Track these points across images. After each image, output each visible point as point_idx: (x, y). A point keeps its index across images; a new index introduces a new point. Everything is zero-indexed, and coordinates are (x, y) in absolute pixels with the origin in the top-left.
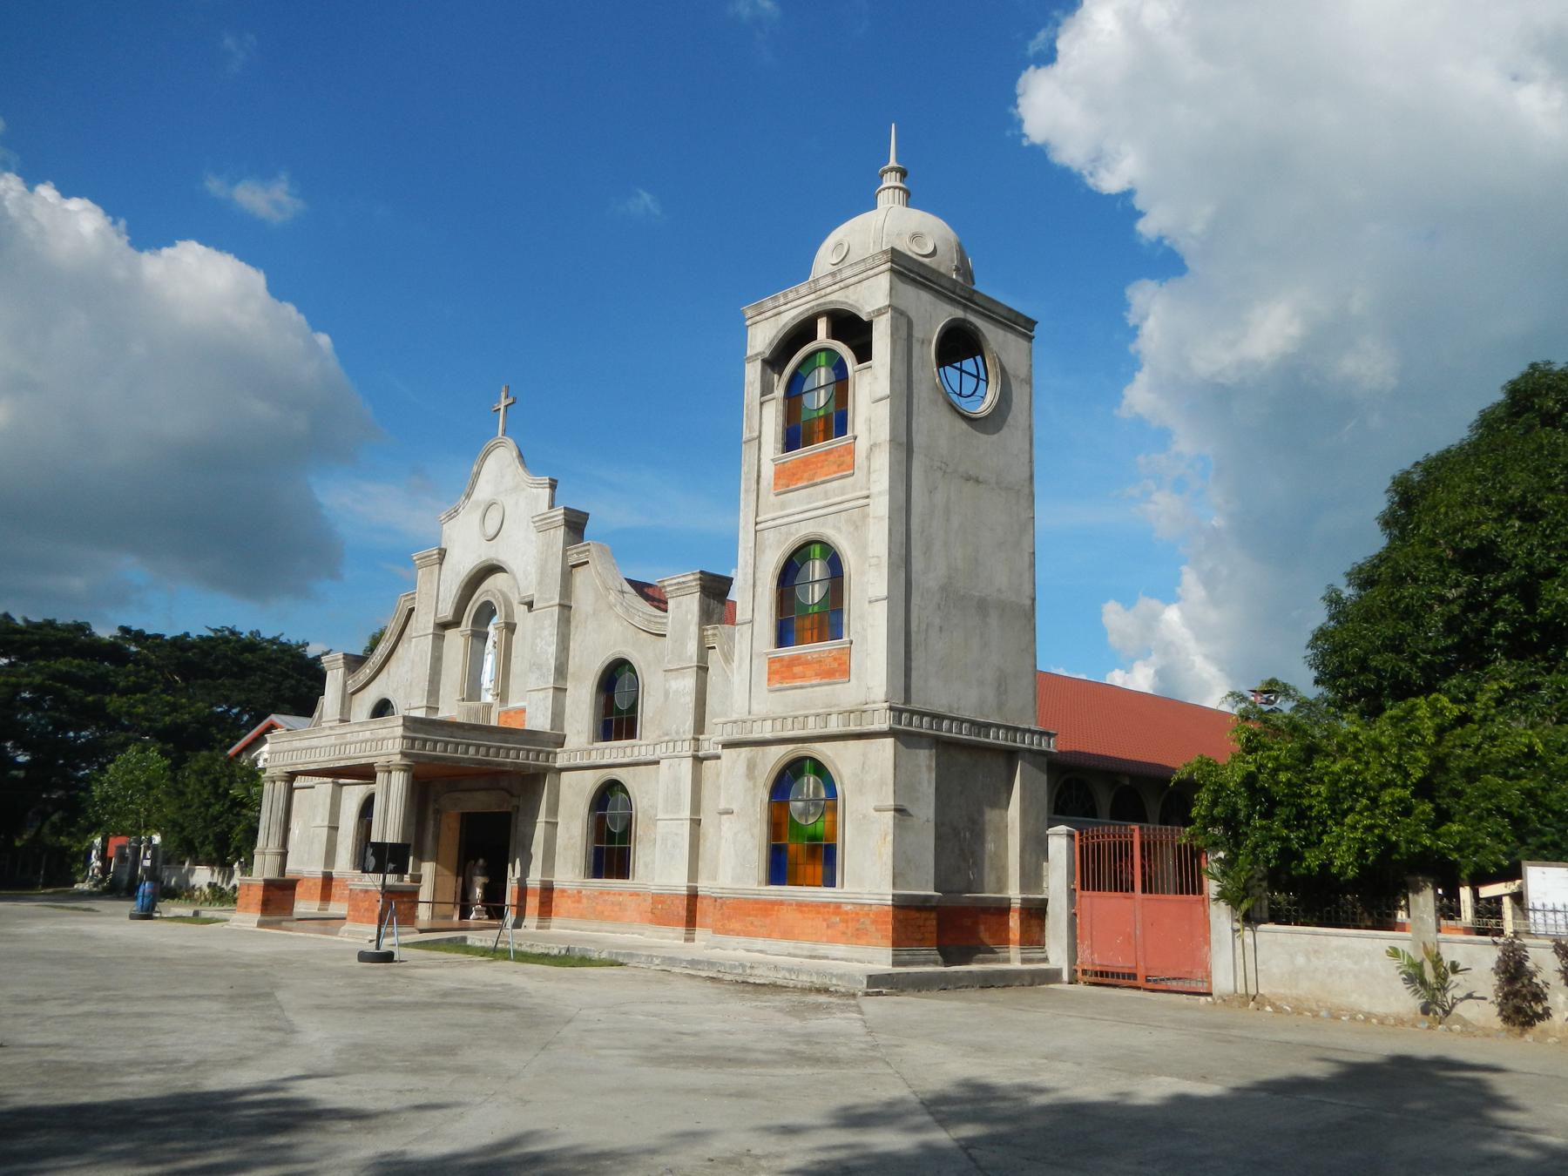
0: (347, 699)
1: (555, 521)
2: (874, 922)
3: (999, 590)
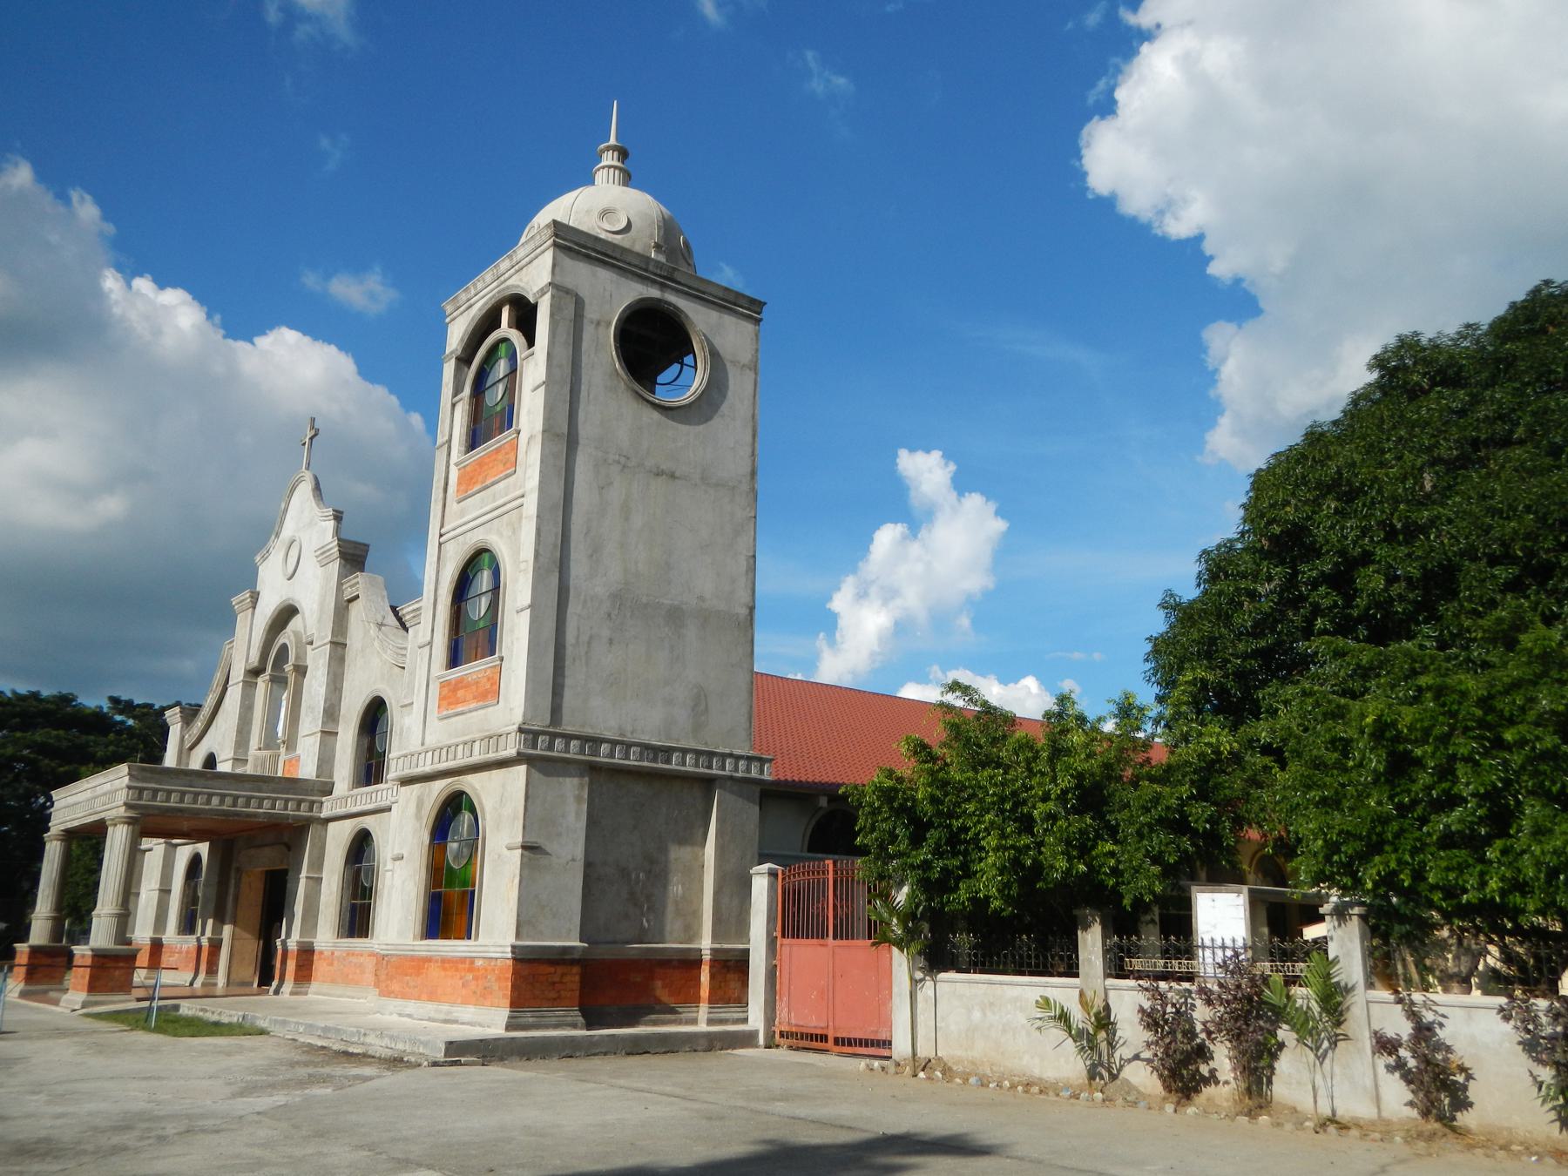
0: (184, 756)
2: (499, 979)
3: (701, 598)
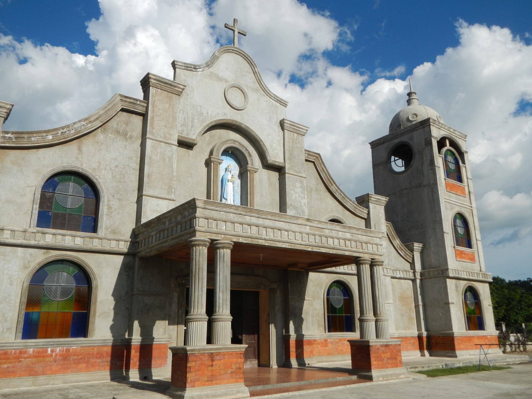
1: (300, 131)
